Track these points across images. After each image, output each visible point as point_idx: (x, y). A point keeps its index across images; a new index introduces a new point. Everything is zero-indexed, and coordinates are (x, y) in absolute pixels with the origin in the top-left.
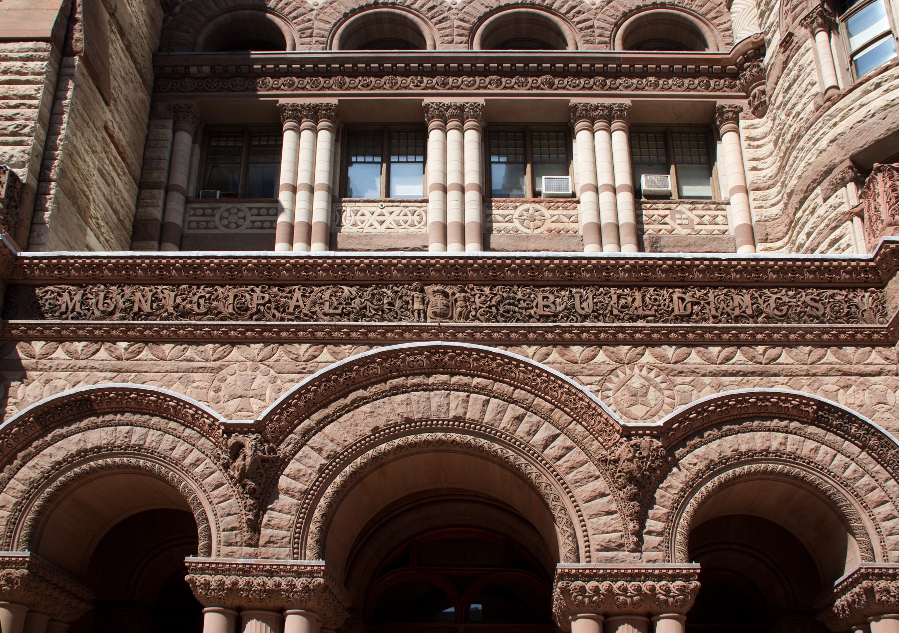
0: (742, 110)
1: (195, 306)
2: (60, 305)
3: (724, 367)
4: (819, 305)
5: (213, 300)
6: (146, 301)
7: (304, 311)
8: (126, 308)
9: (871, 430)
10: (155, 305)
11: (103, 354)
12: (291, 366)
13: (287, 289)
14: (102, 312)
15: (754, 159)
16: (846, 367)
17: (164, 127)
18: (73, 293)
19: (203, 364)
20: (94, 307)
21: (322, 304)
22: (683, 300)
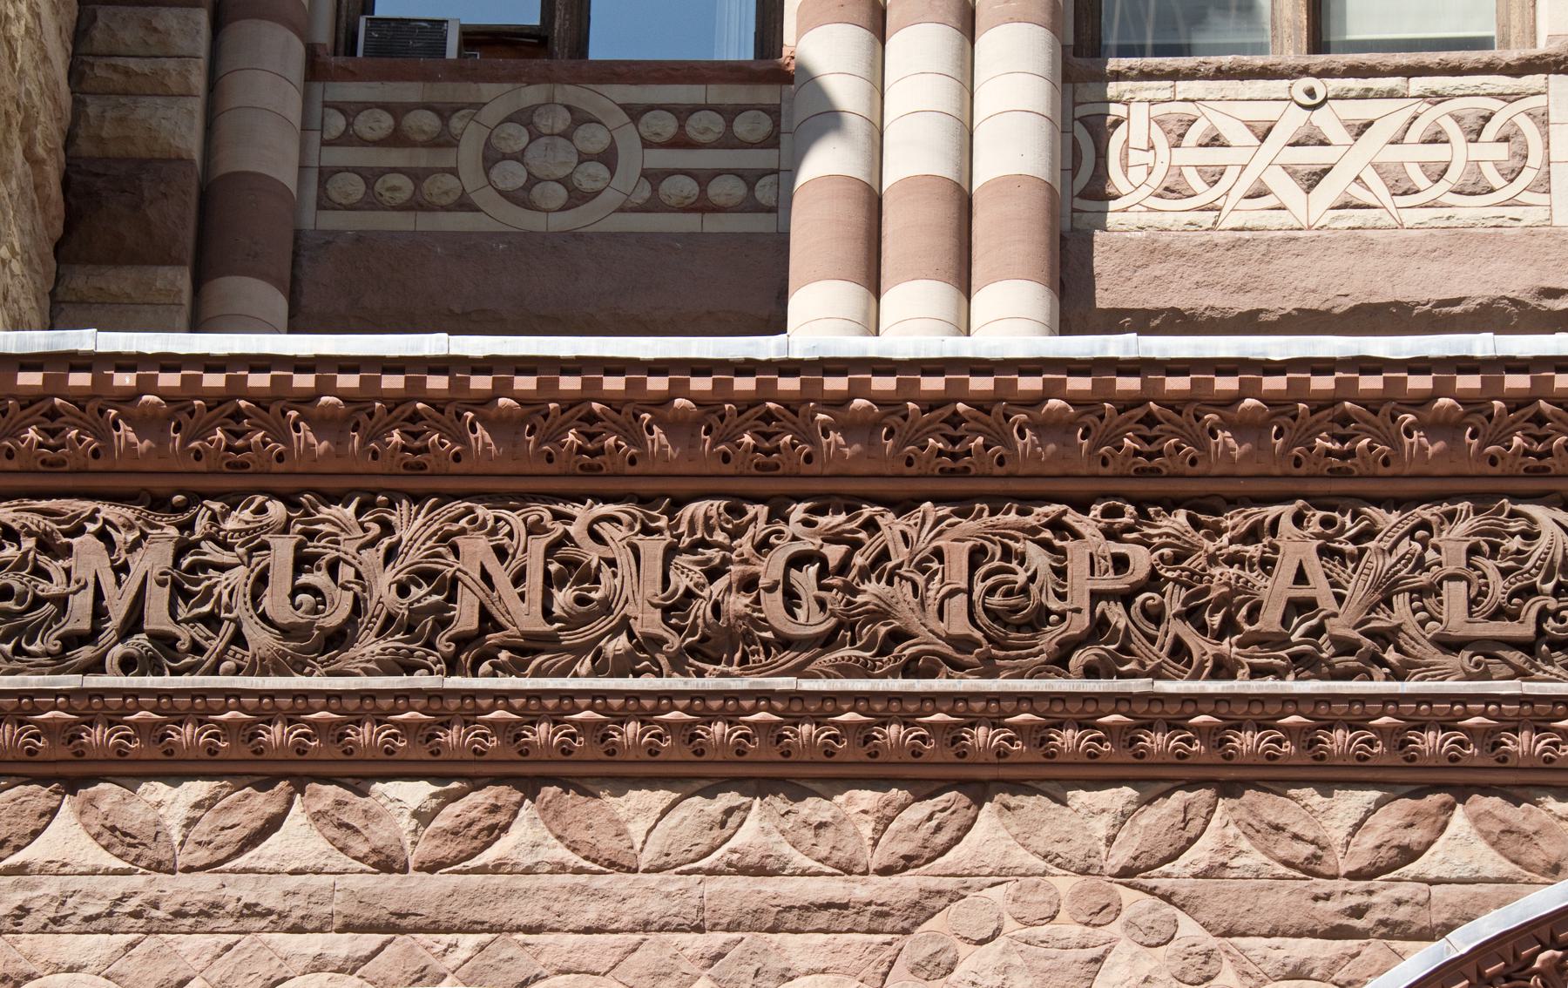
1: (773, 605)
2: (62, 602)
5: (864, 574)
6: (519, 578)
7: (1340, 626)
8: (417, 614)
10: (563, 598)
12: (1289, 898)
13: (1236, 521)
14: (287, 632)
18: (122, 537)
20: (242, 609)
21: (1434, 590)
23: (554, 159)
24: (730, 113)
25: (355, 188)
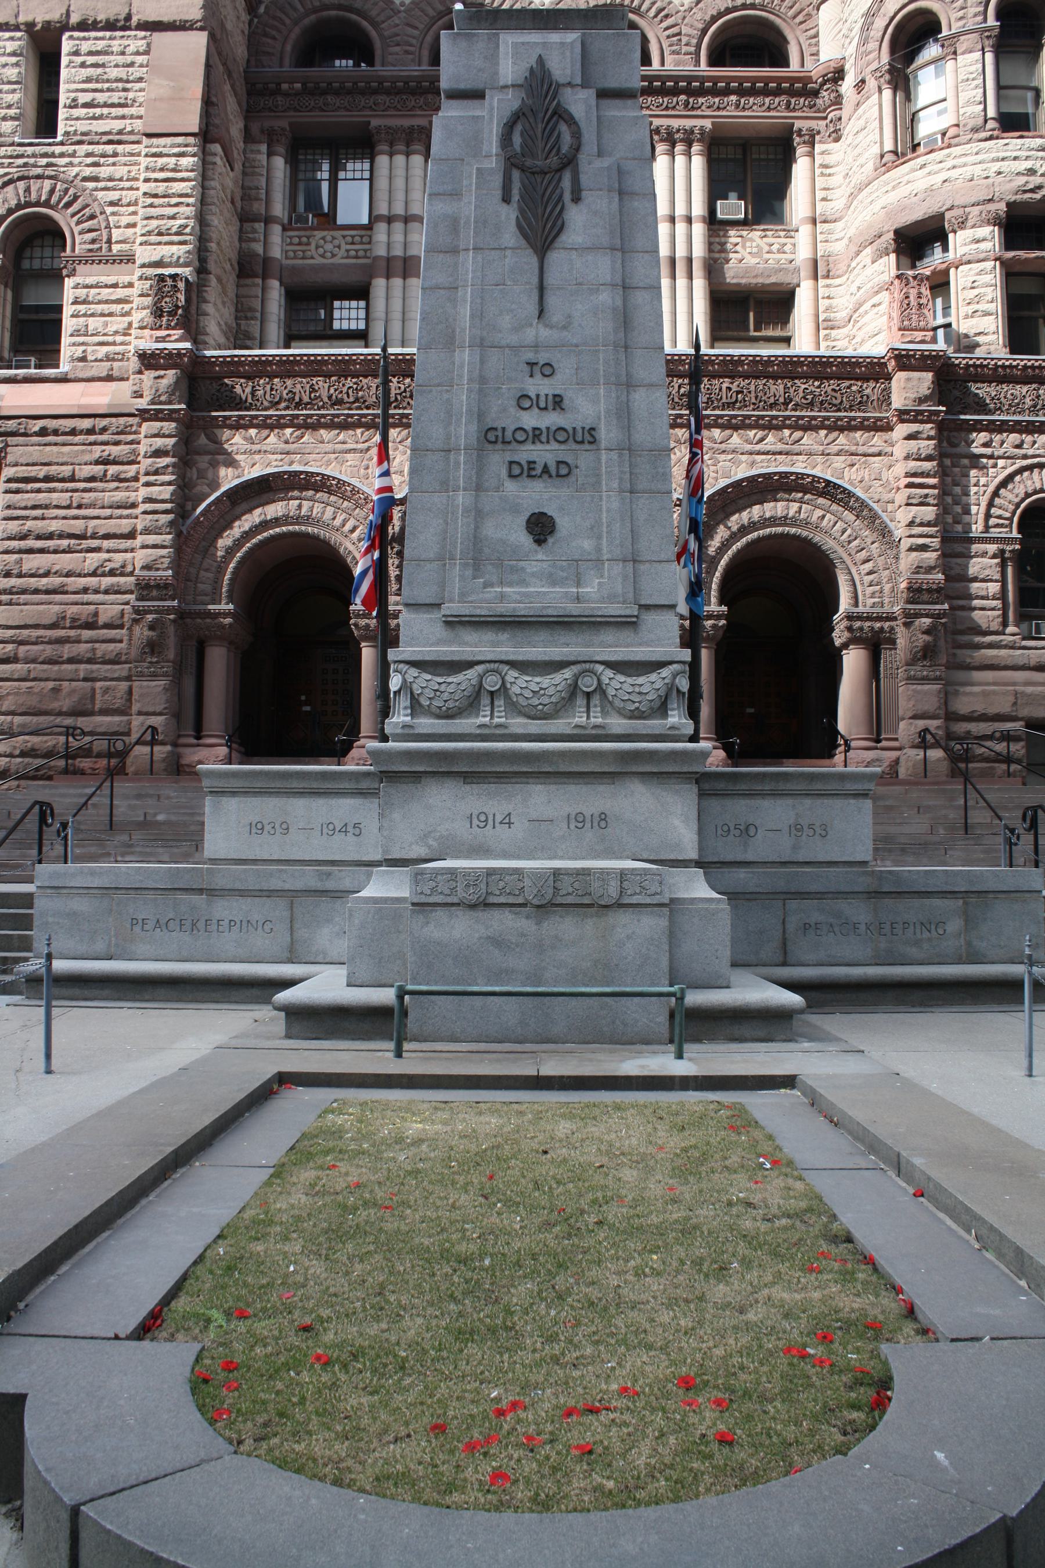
0: (819, 133)
3: (758, 447)
4: (838, 395)
9: (863, 504)
11: (272, 439)
15: (825, 189)
16: (853, 448)
17: (259, 152)
19: (354, 446)
22: (729, 389)
23: (329, 247)
24: (362, 237)
25: (291, 254)
